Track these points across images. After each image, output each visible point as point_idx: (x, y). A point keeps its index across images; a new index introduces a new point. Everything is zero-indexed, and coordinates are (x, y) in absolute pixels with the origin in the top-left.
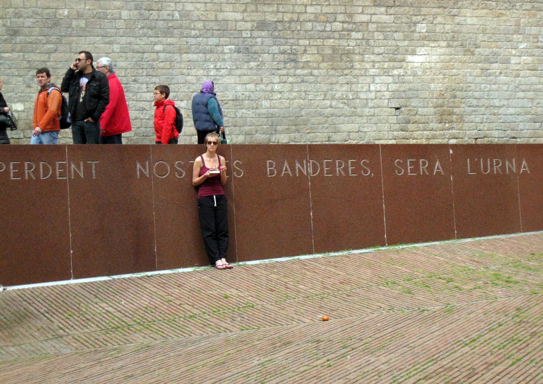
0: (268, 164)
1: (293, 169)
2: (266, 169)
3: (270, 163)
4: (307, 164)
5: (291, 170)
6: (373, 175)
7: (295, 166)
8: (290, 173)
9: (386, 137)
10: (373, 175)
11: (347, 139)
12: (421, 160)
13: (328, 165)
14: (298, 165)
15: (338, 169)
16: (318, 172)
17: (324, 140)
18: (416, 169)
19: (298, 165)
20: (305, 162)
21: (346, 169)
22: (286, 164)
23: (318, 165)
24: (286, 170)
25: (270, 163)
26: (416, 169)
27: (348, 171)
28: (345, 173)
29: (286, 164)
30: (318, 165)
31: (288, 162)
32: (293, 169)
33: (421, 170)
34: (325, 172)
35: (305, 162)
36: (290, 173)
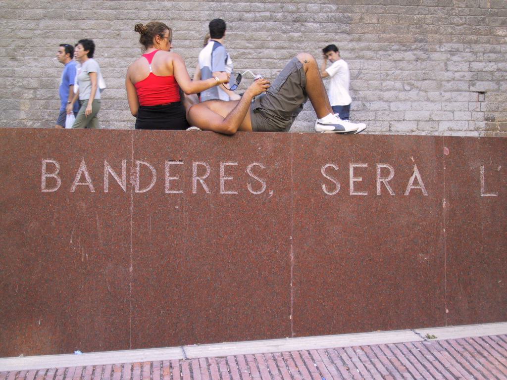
0: (44, 168)
1: (97, 177)
2: (40, 176)
3: (48, 164)
4: (128, 170)
5: (93, 180)
6: (271, 193)
7: (103, 173)
8: (91, 186)
9: (465, 128)
10: (271, 193)
11: (415, 129)
12: (380, 166)
13: (174, 170)
14: (108, 169)
15: (195, 179)
16: (152, 185)
17: (384, 130)
18: (368, 182)
19: (108, 169)
20: (124, 165)
21: (213, 182)
22: (83, 167)
23: (154, 171)
24: (83, 179)
25: (48, 164)
26: (368, 182)
27: (218, 185)
28: (211, 190)
29: (83, 167)
30: (154, 171)
31: (87, 164)
32: (97, 177)
33: (378, 186)
34: (167, 185)
35: (124, 165)
36: (91, 186)
